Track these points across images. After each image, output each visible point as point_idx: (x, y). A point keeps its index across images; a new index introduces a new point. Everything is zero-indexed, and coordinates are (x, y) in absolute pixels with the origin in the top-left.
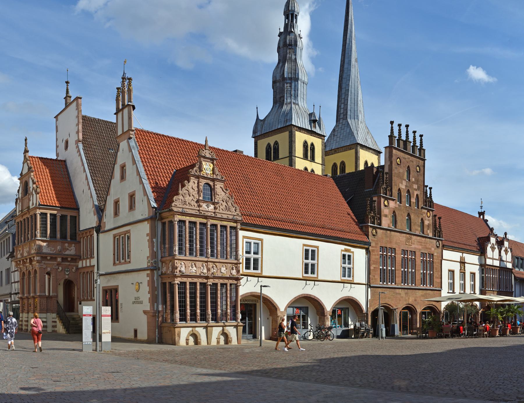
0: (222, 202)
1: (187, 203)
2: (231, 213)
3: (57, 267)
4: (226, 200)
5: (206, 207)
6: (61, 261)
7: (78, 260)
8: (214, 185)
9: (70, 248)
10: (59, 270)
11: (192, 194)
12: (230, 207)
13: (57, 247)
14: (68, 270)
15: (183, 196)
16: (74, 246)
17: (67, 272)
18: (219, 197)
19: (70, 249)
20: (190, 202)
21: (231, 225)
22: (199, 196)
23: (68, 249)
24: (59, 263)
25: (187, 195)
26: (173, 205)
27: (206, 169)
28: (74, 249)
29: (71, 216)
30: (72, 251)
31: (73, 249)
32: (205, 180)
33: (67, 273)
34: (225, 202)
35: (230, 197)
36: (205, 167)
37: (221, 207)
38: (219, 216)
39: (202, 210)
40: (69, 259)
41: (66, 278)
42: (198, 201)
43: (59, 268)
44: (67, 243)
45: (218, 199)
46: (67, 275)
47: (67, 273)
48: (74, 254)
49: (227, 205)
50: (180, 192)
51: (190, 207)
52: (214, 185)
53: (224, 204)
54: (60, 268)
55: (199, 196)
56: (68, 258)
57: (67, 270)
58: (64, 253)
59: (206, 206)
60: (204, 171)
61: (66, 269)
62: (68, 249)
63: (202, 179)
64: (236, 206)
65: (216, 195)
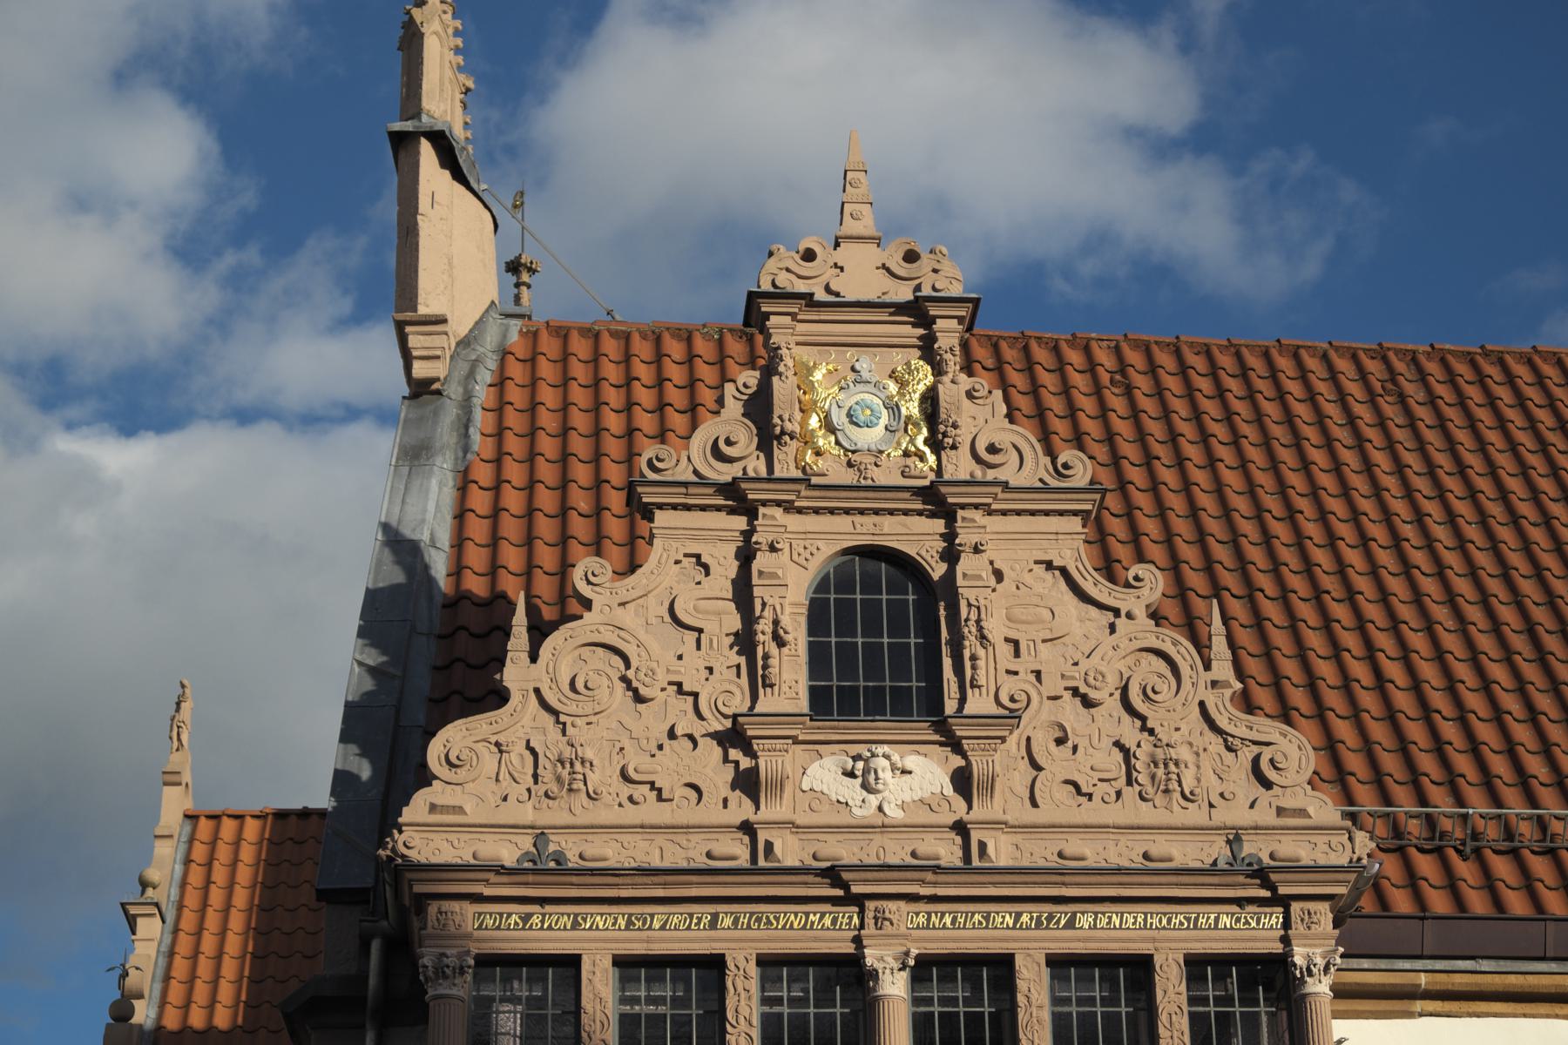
0: (1070, 711)
1: (603, 777)
2: (1195, 815)
4: (1125, 690)
5: (851, 791)
8: (951, 555)
11: (662, 678)
12: (1184, 753)
15: (555, 713)
18: (1025, 664)
20: (636, 762)
21: (1199, 948)
22: (758, 679)
25: (602, 694)
26: (416, 809)
27: (839, 418)
32: (842, 523)
34: (1113, 705)
35: (1184, 653)
36: (825, 392)
37: (1057, 763)
38: (1002, 851)
39: (793, 826)
42: (734, 737)
45: (1008, 686)
49: (1129, 732)
50: (516, 673)
51: (651, 811)
52: (951, 555)
53: (1111, 721)
55: (758, 679)
59: (851, 774)
60: (824, 441)
63: (788, 507)
64: (1268, 729)
65: (971, 645)
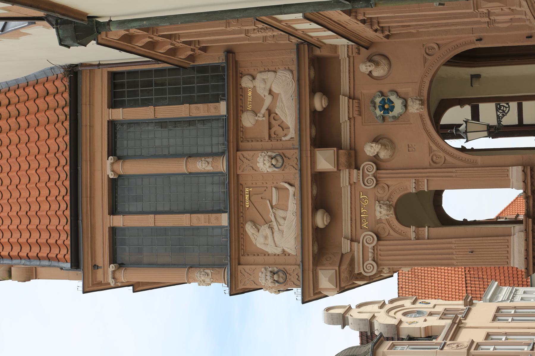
3: (369, 167)
6: (330, 152)
7: (318, 52)
9: (263, 101)
10: (384, 154)
13: (262, 174)
14: (378, 100)
16: (254, 78)
17: (392, 108)
19: (268, 100)
23: (270, 112)
24: (343, 160)
28: (265, 76)
29: (113, 104)
30: (275, 90)
31: (264, 80)
33: (398, 103)
40: (319, 103)
41: (425, 112)
43: (376, 160)
44: (238, 120)
46: (406, 106)
47: (398, 103)
48: (288, 75)
54: (371, 149)
56: (314, 112)
57: (382, 108)
58: (292, 133)
61: (379, 112)
62: (270, 112)
